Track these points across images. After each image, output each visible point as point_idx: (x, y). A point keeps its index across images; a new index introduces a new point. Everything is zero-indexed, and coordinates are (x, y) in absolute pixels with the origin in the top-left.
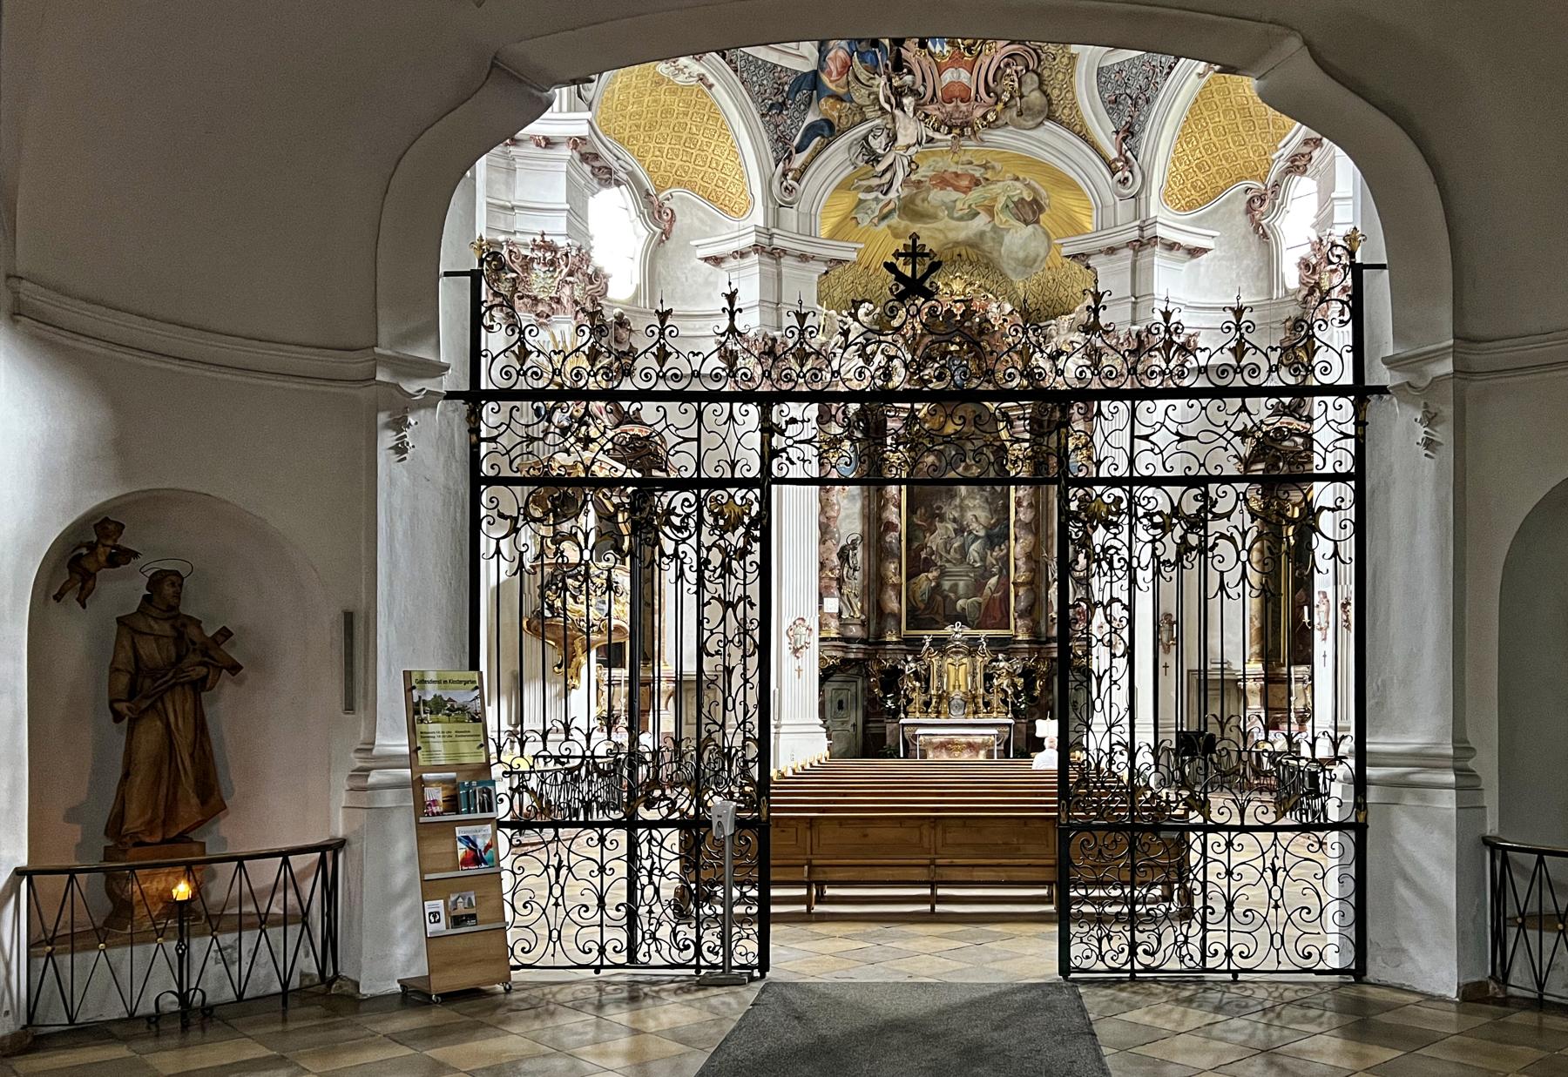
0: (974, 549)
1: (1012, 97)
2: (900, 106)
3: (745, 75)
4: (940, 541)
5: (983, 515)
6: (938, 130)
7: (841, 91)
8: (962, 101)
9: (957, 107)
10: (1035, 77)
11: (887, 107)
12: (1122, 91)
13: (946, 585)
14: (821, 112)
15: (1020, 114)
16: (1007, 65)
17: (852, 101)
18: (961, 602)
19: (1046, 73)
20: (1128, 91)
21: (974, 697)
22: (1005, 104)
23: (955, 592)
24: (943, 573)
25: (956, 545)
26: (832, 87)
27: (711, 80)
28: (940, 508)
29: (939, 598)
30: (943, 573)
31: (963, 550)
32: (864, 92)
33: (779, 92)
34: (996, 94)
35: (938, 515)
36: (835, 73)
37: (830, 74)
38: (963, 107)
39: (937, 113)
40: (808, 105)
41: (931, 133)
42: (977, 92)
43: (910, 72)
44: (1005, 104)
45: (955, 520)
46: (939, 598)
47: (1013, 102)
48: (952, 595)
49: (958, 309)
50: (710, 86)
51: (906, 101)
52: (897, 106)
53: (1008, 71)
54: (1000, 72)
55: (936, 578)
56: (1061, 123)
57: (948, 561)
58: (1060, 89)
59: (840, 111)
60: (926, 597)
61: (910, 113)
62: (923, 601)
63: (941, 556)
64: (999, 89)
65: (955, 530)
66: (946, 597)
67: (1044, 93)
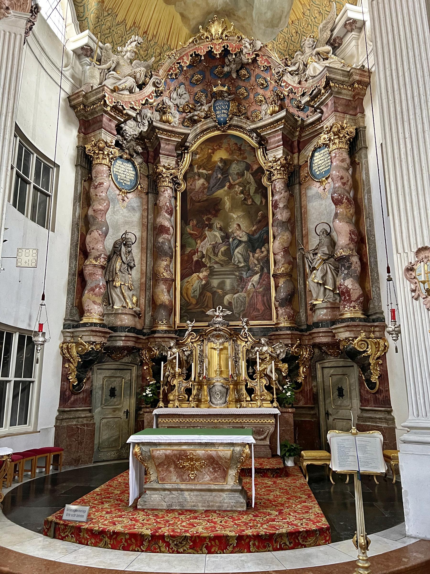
0: (238, 252)
4: (208, 246)
5: (244, 224)
13: (215, 282)
18: (227, 297)
21: (236, 384)
23: (222, 289)
24: (212, 273)
25: (223, 249)
28: (209, 219)
29: (209, 294)
30: (212, 273)
31: (229, 254)
35: (207, 225)
45: (221, 229)
46: (209, 294)
48: (220, 291)
49: (217, 51)
55: (206, 277)
57: (216, 263)
60: (197, 293)
62: (194, 297)
63: (210, 259)
65: (222, 237)
66: (214, 293)
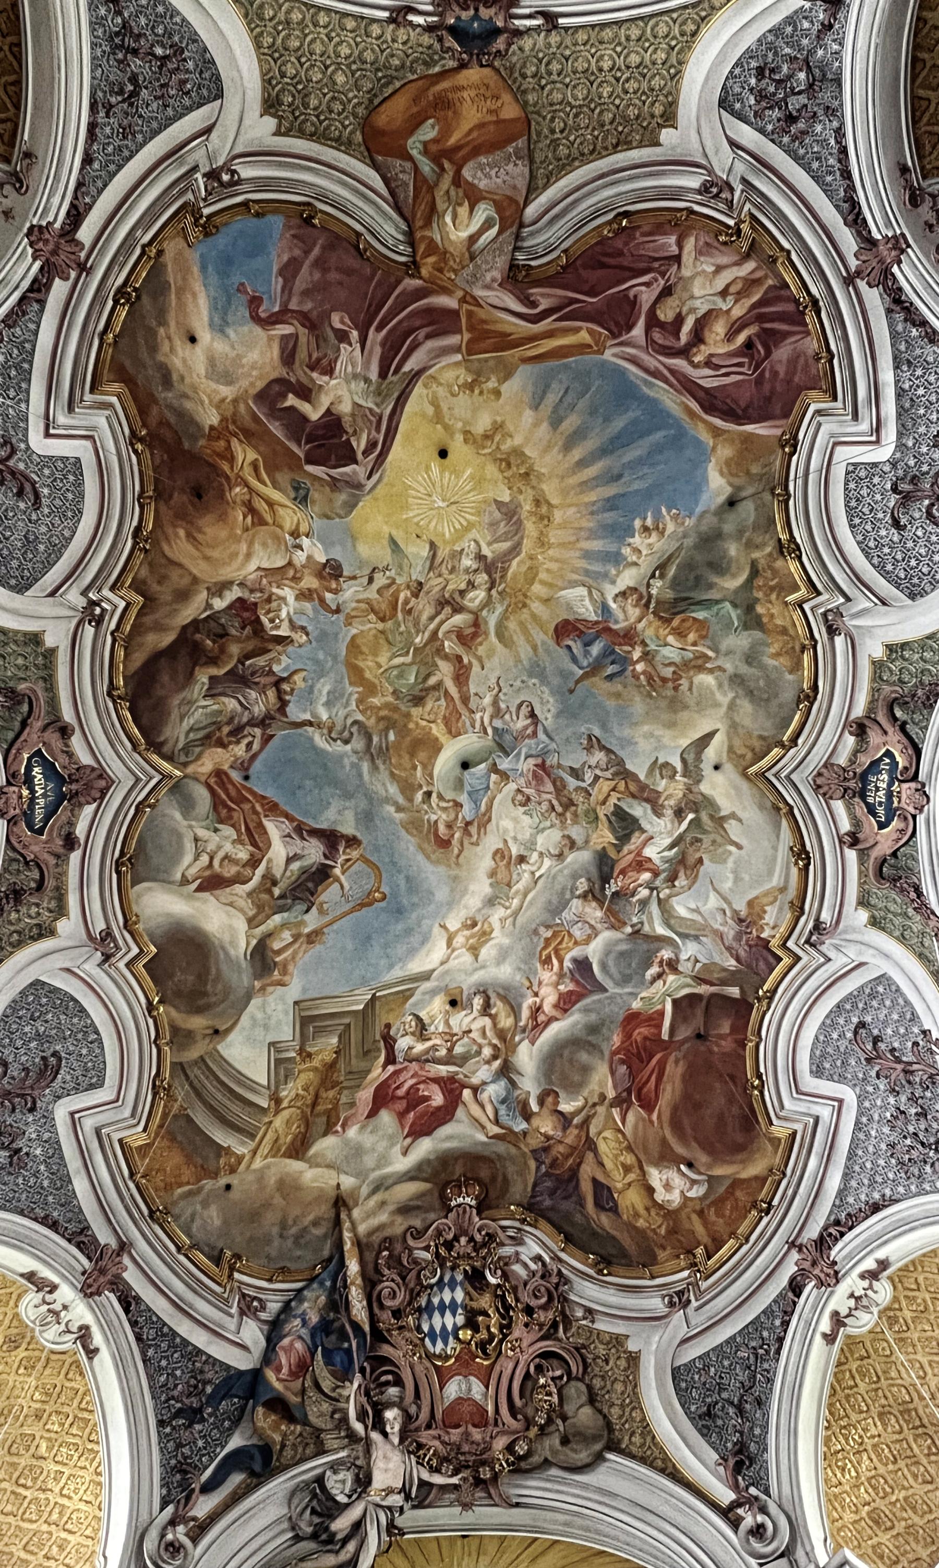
1: (550, 1421)
2: (379, 1425)
3: (151, 1352)
6: (437, 1470)
7: (294, 1399)
8: (475, 1426)
9: (467, 1434)
10: (583, 1388)
11: (358, 1427)
12: (716, 1397)
14: (256, 1431)
15: (565, 1441)
16: (539, 1369)
17: (306, 1422)
19: (597, 1383)
20: (725, 1395)
22: (542, 1428)
26: (278, 1386)
27: (98, 1339)
32: (326, 1407)
33: (194, 1390)
34: (526, 1418)
36: (285, 1370)
37: (278, 1370)
38: (477, 1434)
39: (437, 1443)
40: (236, 1423)
41: (425, 1475)
42: (497, 1411)
43: (398, 1382)
44: (542, 1428)
47: (552, 1428)
50: (92, 1353)
51: (390, 1414)
52: (374, 1427)
53: (542, 1381)
54: (529, 1384)
56: (632, 1456)
58: (622, 1406)
59: (284, 1435)
61: (396, 1440)
64: (530, 1411)
67: (600, 1411)
